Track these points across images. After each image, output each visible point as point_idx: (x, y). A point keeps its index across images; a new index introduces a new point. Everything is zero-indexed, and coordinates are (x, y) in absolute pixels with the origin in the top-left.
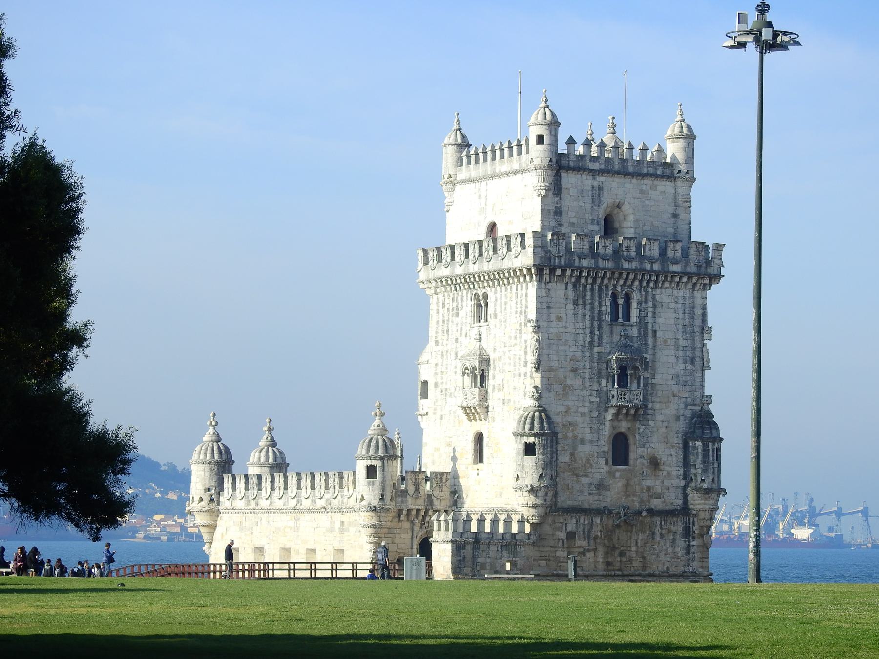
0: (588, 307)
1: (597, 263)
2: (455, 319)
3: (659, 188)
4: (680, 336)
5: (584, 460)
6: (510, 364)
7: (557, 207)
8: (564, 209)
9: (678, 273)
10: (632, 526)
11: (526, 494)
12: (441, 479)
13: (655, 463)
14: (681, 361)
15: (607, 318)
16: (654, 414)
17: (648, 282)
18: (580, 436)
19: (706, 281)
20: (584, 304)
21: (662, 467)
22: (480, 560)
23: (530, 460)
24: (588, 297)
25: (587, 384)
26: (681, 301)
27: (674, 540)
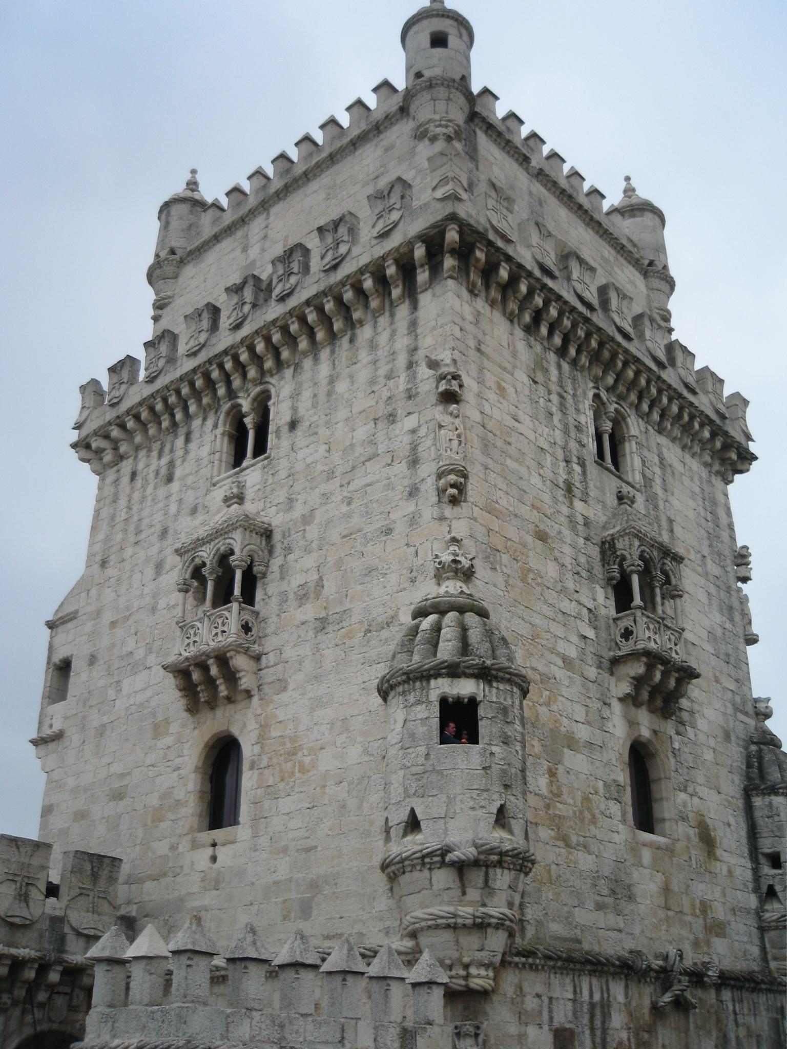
2: (162, 492)
3: (626, 270)
4: (706, 551)
6: (348, 516)
11: (443, 878)
12: (95, 877)
13: (708, 841)
15: (592, 446)
18: (565, 721)
21: (719, 852)
23: (464, 758)
25: (570, 585)
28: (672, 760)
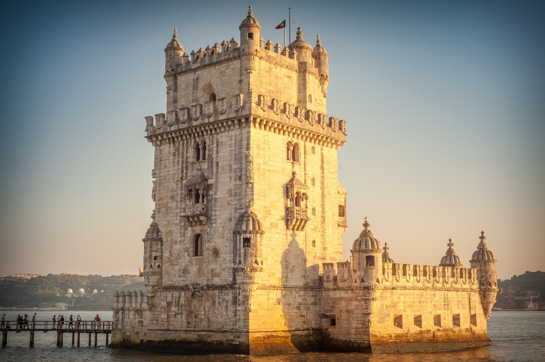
0: (180, 156)
1: (178, 126)
3: (232, 67)
4: (232, 162)
5: (177, 254)
7: (175, 99)
8: (179, 98)
9: (223, 120)
10: (202, 296)
13: (216, 252)
14: (233, 179)
16: (215, 219)
17: (211, 130)
19: (243, 120)
20: (179, 155)
21: (220, 255)
22: (125, 320)
24: (181, 149)
25: (179, 205)
26: (234, 138)
27: (227, 306)
28: (206, 236)
